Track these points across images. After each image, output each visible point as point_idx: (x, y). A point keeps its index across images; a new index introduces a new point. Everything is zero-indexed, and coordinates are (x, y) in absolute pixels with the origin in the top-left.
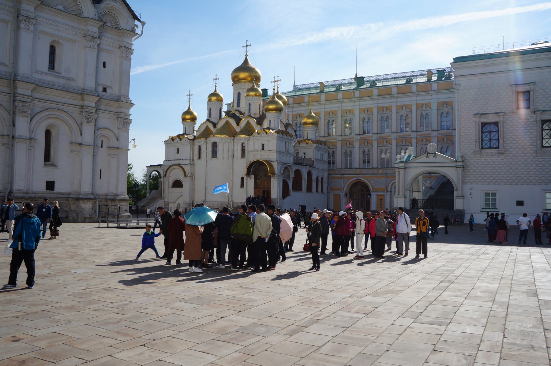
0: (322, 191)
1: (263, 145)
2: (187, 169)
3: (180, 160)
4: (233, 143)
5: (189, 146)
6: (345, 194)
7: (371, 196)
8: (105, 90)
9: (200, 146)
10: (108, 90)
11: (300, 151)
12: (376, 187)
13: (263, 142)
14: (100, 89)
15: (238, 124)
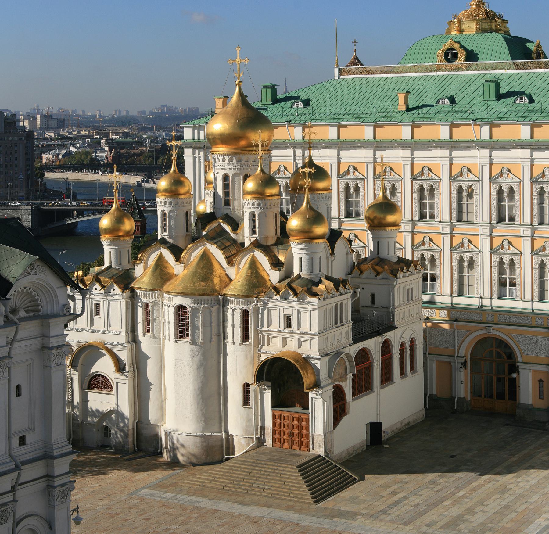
0: (412, 368)
1: (288, 319)
2: (124, 356)
3: (103, 332)
4: (223, 307)
5: (124, 303)
6: (462, 364)
7: (519, 373)
8: (22, 441)
9: (147, 305)
10: (28, 440)
11: (363, 289)
12: (528, 353)
13: (288, 312)
14: (16, 441)
15: (230, 262)
